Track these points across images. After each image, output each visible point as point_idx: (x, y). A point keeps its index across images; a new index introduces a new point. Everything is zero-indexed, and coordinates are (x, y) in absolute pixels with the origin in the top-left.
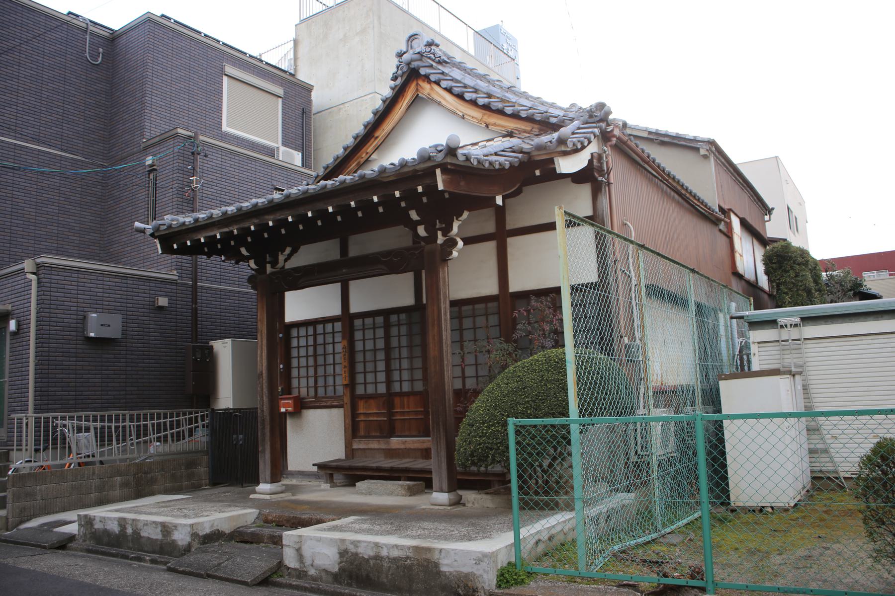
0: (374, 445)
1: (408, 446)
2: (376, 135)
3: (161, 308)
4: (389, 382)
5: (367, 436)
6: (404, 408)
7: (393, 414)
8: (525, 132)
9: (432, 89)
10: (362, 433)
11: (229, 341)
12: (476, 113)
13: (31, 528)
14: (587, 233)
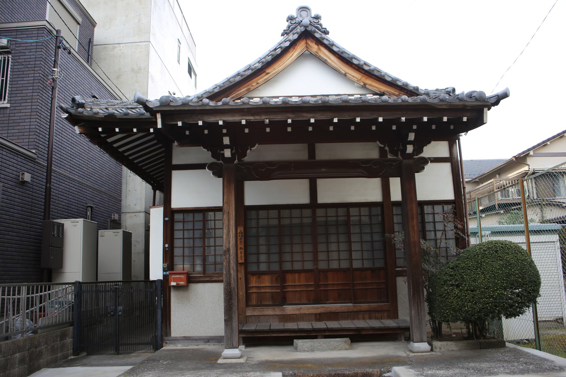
0: (269, 311)
1: (302, 312)
2: (268, 71)
3: (24, 183)
4: (281, 262)
5: (260, 305)
6: (295, 282)
7: (284, 287)
8: (394, 94)
9: (319, 49)
10: (254, 302)
11: (81, 221)
12: (356, 75)
13: (524, 352)
14: (446, 167)
